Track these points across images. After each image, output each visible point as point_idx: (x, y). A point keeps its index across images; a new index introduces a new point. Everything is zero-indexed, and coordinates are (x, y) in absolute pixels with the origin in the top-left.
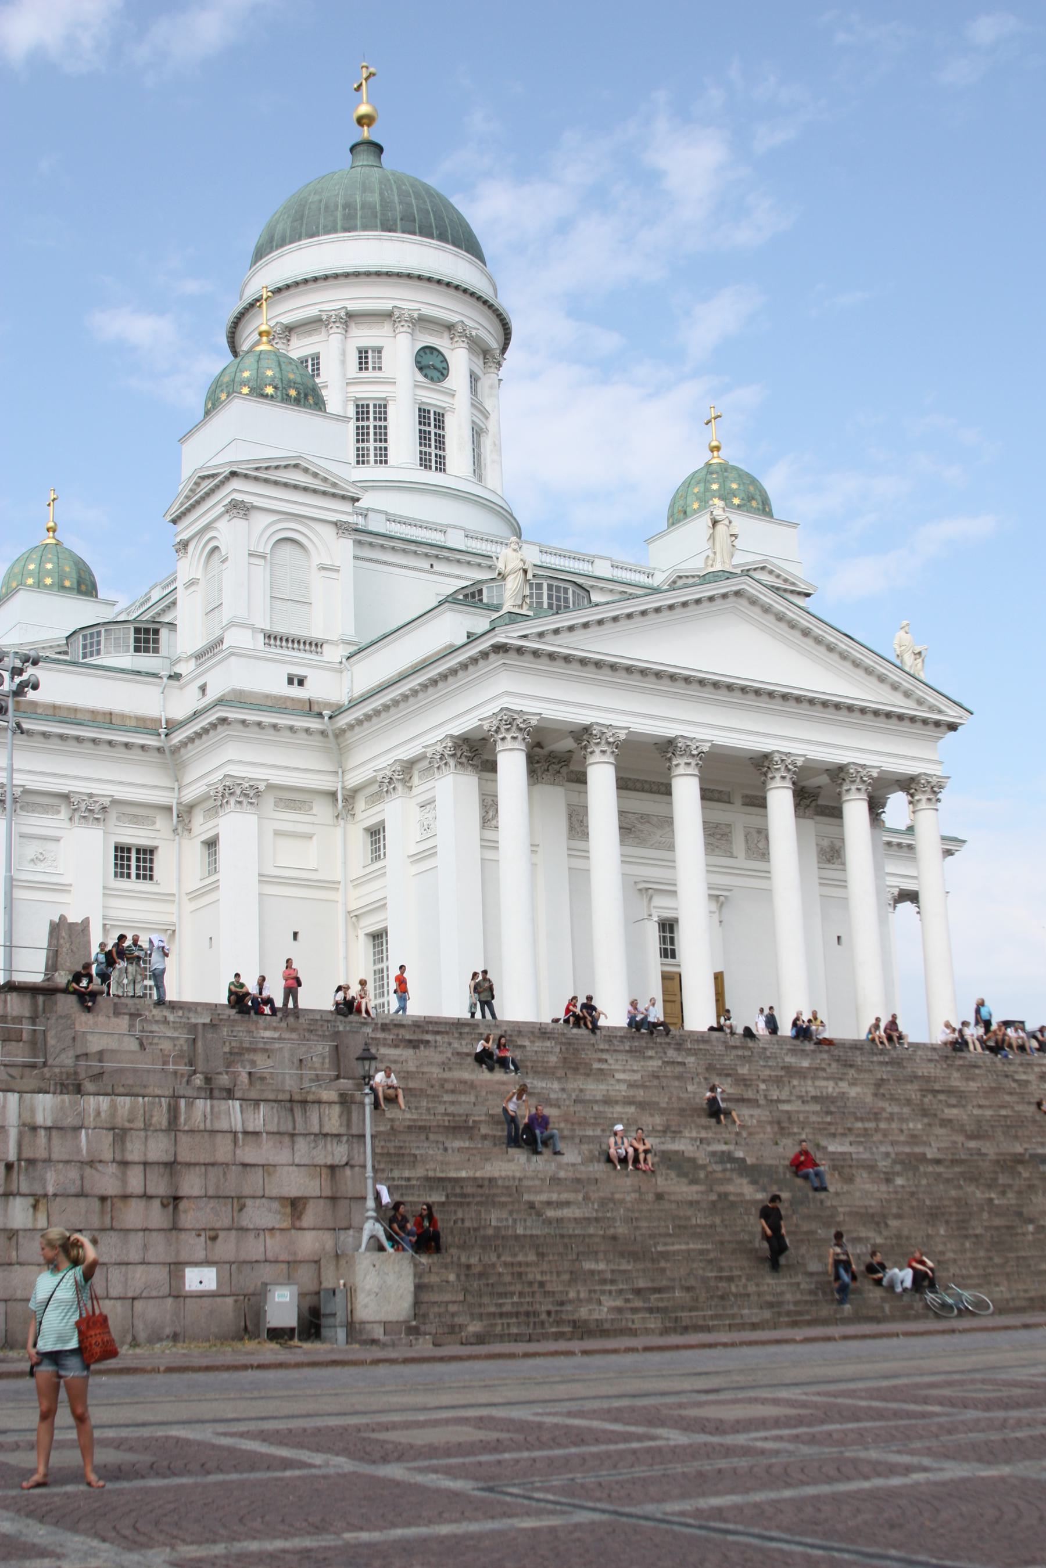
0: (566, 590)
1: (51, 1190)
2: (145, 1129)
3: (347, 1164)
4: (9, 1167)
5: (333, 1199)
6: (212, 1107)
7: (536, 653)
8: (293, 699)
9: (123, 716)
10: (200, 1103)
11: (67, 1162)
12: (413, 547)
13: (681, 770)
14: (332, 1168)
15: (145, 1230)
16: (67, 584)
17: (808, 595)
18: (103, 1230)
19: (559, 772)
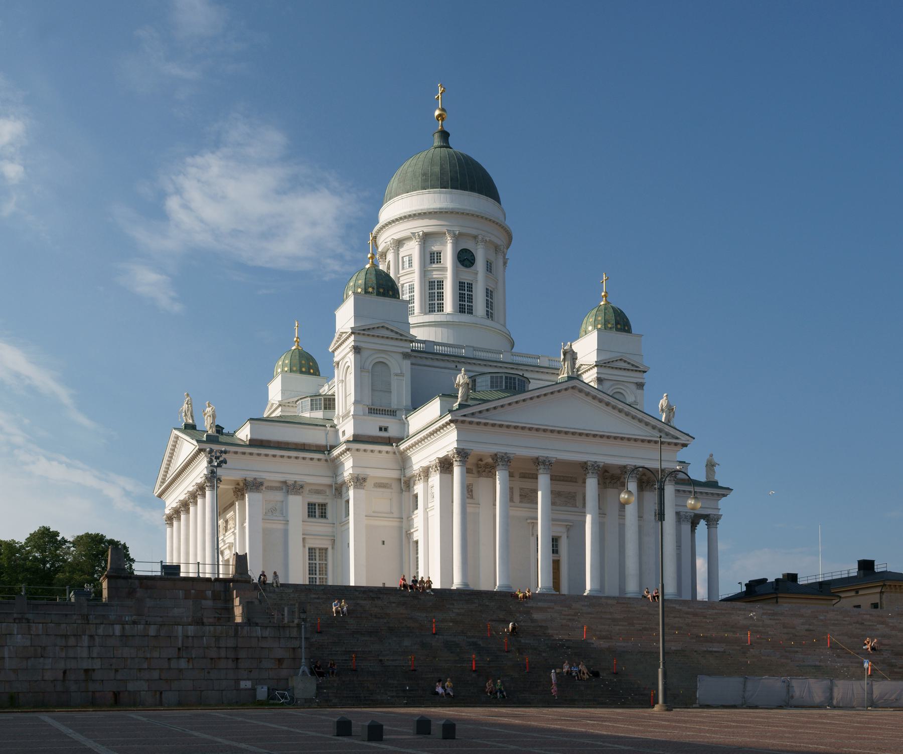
0: (514, 379)
1: (194, 656)
2: (226, 637)
3: (299, 647)
4: (179, 649)
5: (294, 659)
6: (250, 629)
7: (471, 423)
8: (381, 437)
9: (309, 445)
10: (245, 627)
11: (200, 647)
12: (447, 358)
13: (541, 471)
14: (294, 649)
15: (226, 669)
16: (304, 369)
17: (645, 372)
18: (212, 669)
19: (490, 472)
